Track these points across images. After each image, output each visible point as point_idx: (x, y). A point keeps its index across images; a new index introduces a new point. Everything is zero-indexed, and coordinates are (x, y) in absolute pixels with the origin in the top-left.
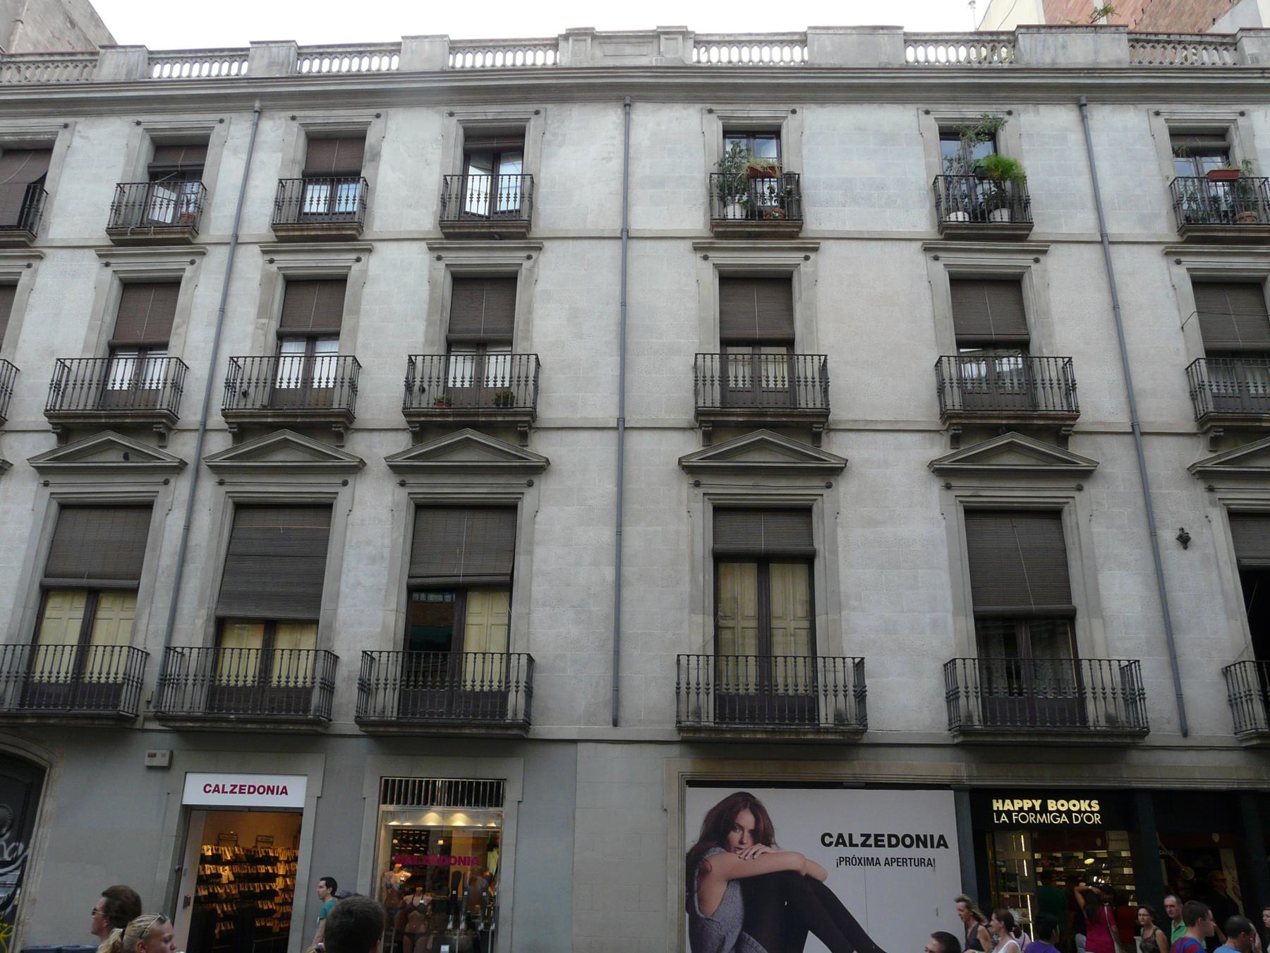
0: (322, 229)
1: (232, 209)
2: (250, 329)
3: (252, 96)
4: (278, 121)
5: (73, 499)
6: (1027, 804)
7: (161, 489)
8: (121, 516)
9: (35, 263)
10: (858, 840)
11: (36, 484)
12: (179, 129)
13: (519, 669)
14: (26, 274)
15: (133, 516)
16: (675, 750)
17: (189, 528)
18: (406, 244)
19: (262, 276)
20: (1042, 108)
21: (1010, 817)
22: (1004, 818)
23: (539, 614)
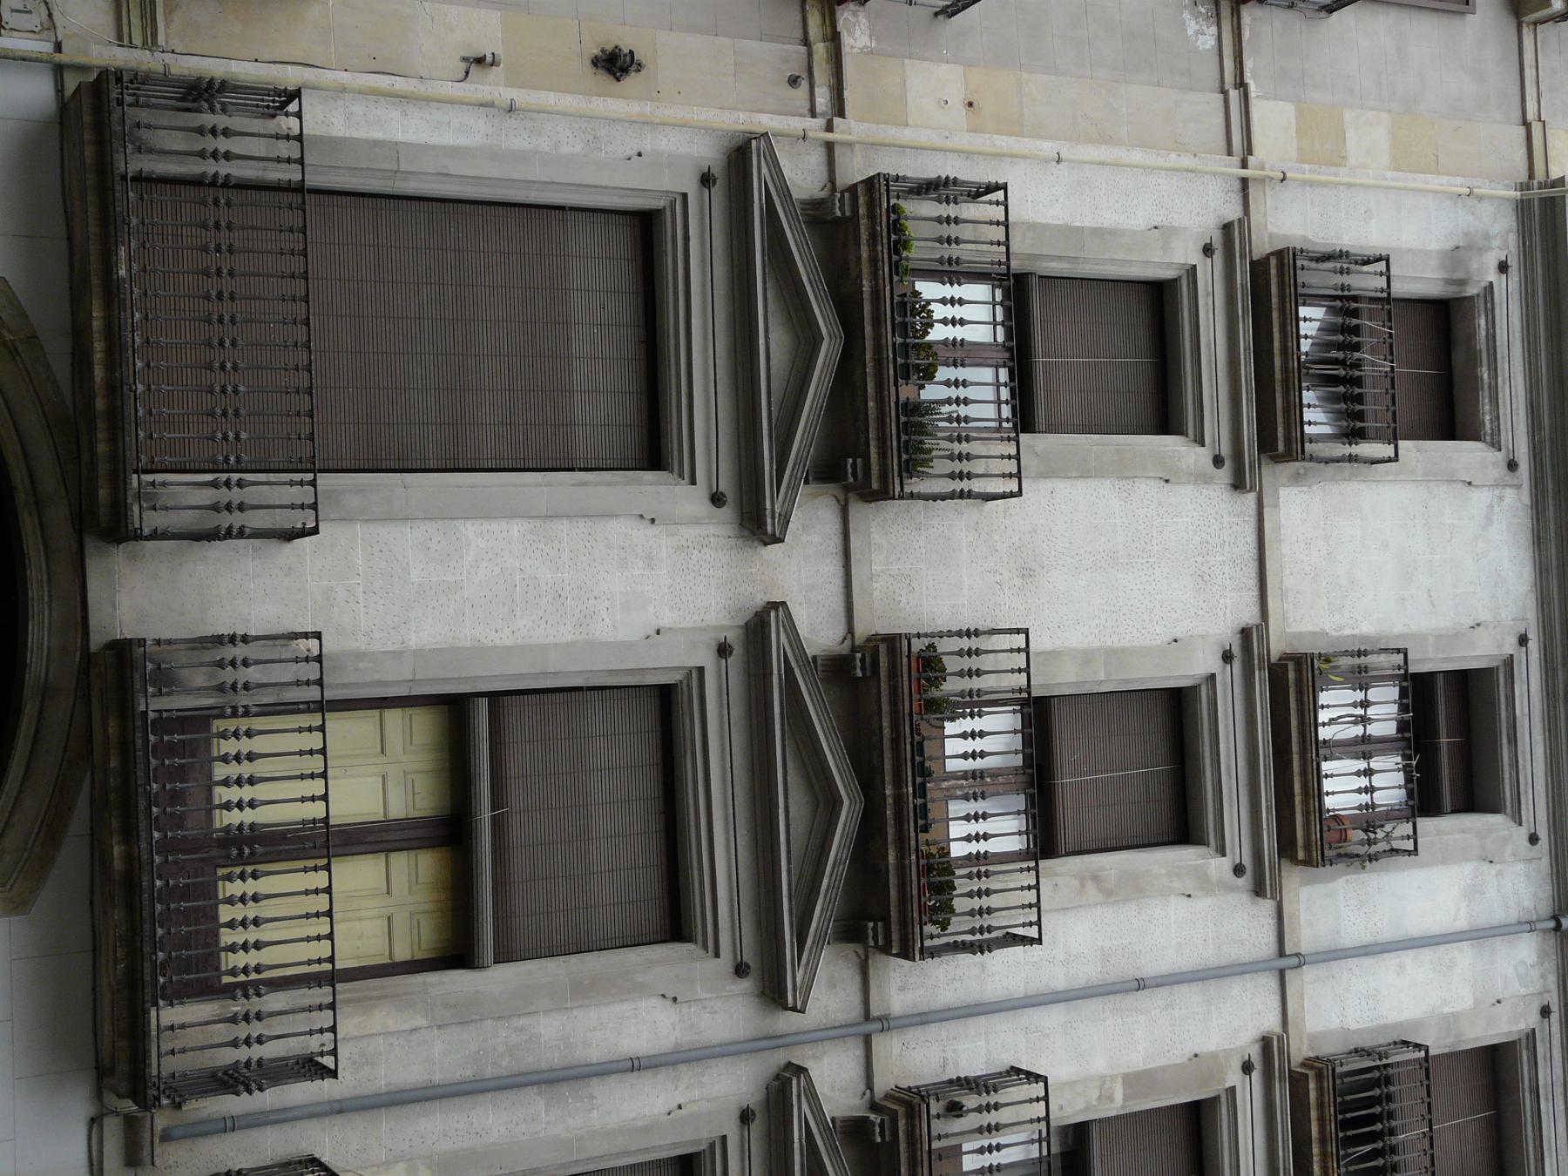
1: (1356, 930)
2: (1099, 1065)
4: (1535, 973)
7: (726, 961)
12: (1513, 740)
14: (1203, 455)
15: (648, 883)
19: (1214, 1056)
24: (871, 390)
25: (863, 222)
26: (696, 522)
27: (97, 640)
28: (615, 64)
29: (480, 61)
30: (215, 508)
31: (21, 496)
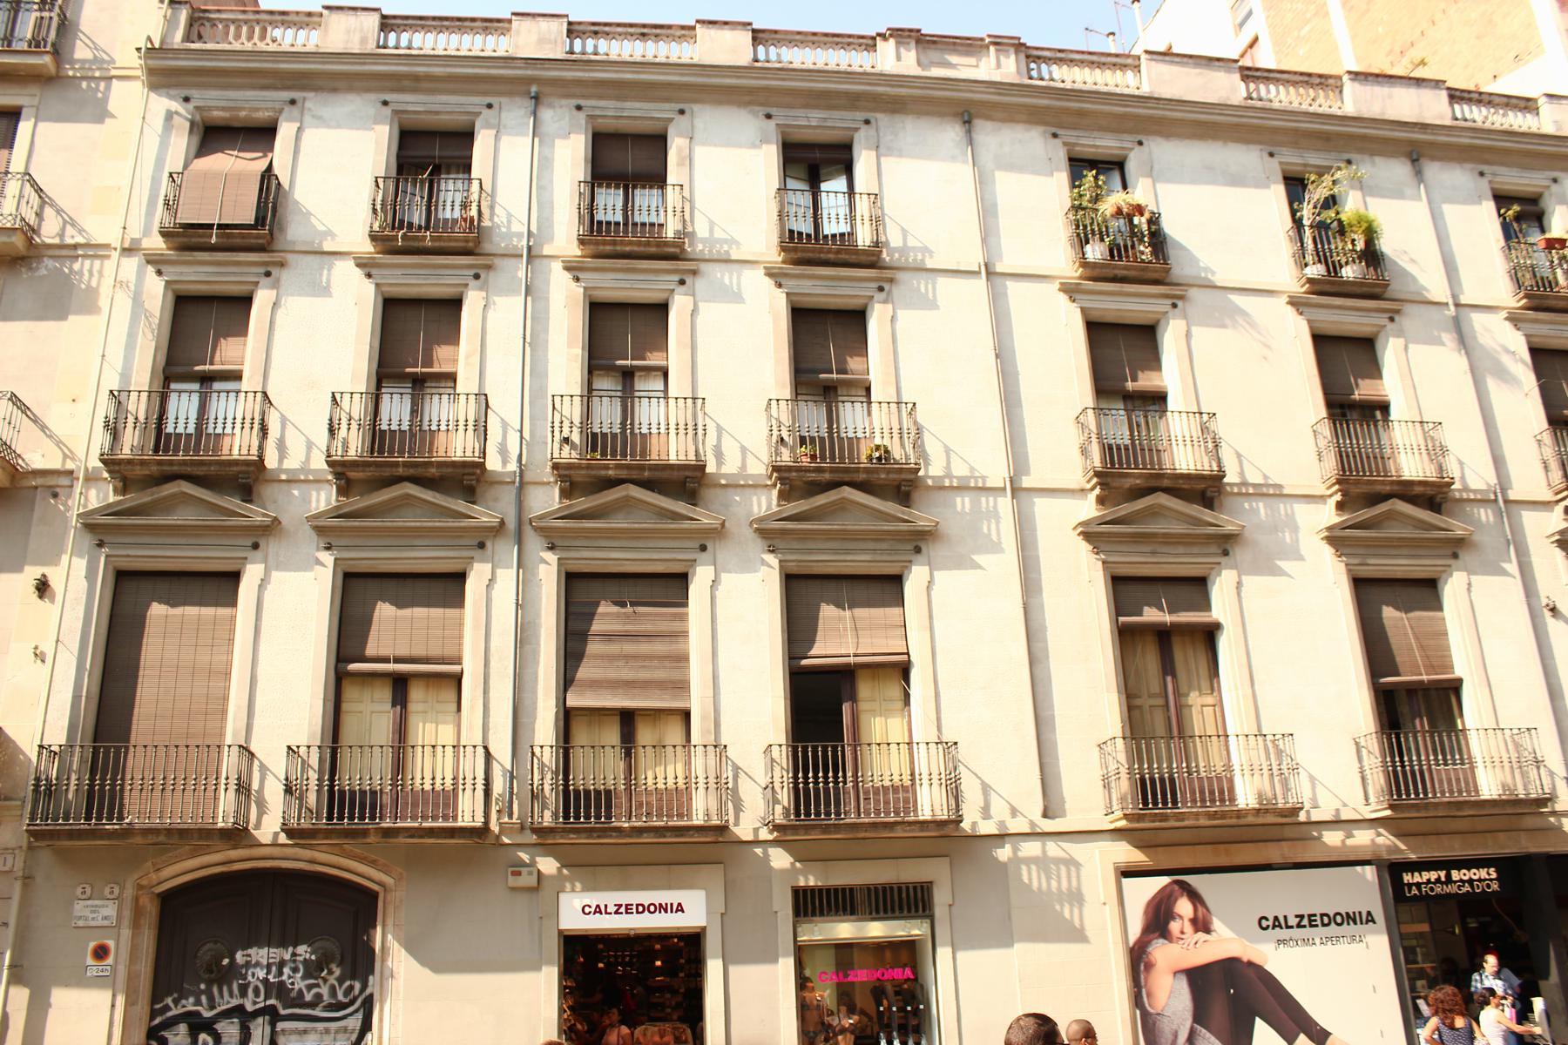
3: (531, 80)
4: (559, 111)
5: (363, 567)
6: (1433, 875)
9: (275, 271)
10: (1293, 921)
12: (437, 113)
20: (1377, 159)
21: (1419, 889)
22: (1415, 891)
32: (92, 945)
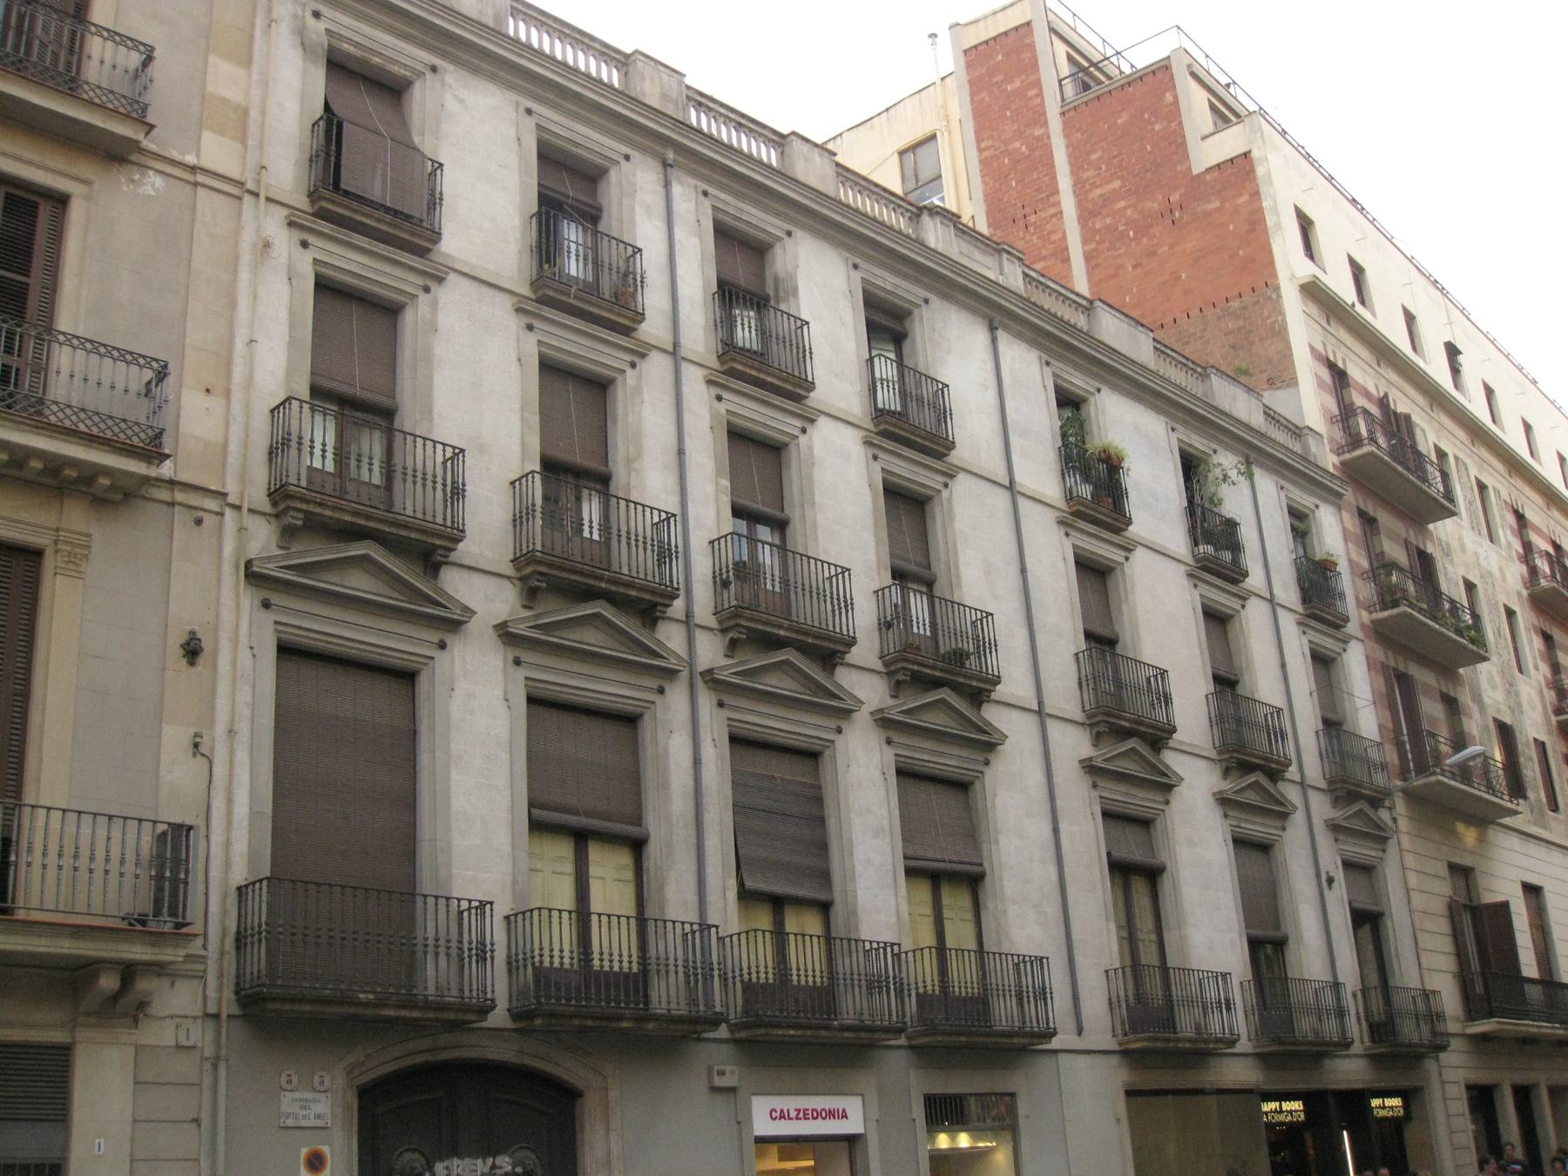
0: (779, 378)
2: (710, 489)
8: (595, 727)
11: (500, 657)
12: (577, 145)
13: (1001, 974)
15: (612, 731)
16: (1114, 1060)
17: (687, 756)
18: (842, 426)
23: (1013, 912)
24: (404, 533)
25: (311, 508)
26: (453, 661)
27: (510, 1025)
28: (192, 651)
29: (196, 745)
30: (448, 955)
31: (429, 1057)
32: (304, 1151)
